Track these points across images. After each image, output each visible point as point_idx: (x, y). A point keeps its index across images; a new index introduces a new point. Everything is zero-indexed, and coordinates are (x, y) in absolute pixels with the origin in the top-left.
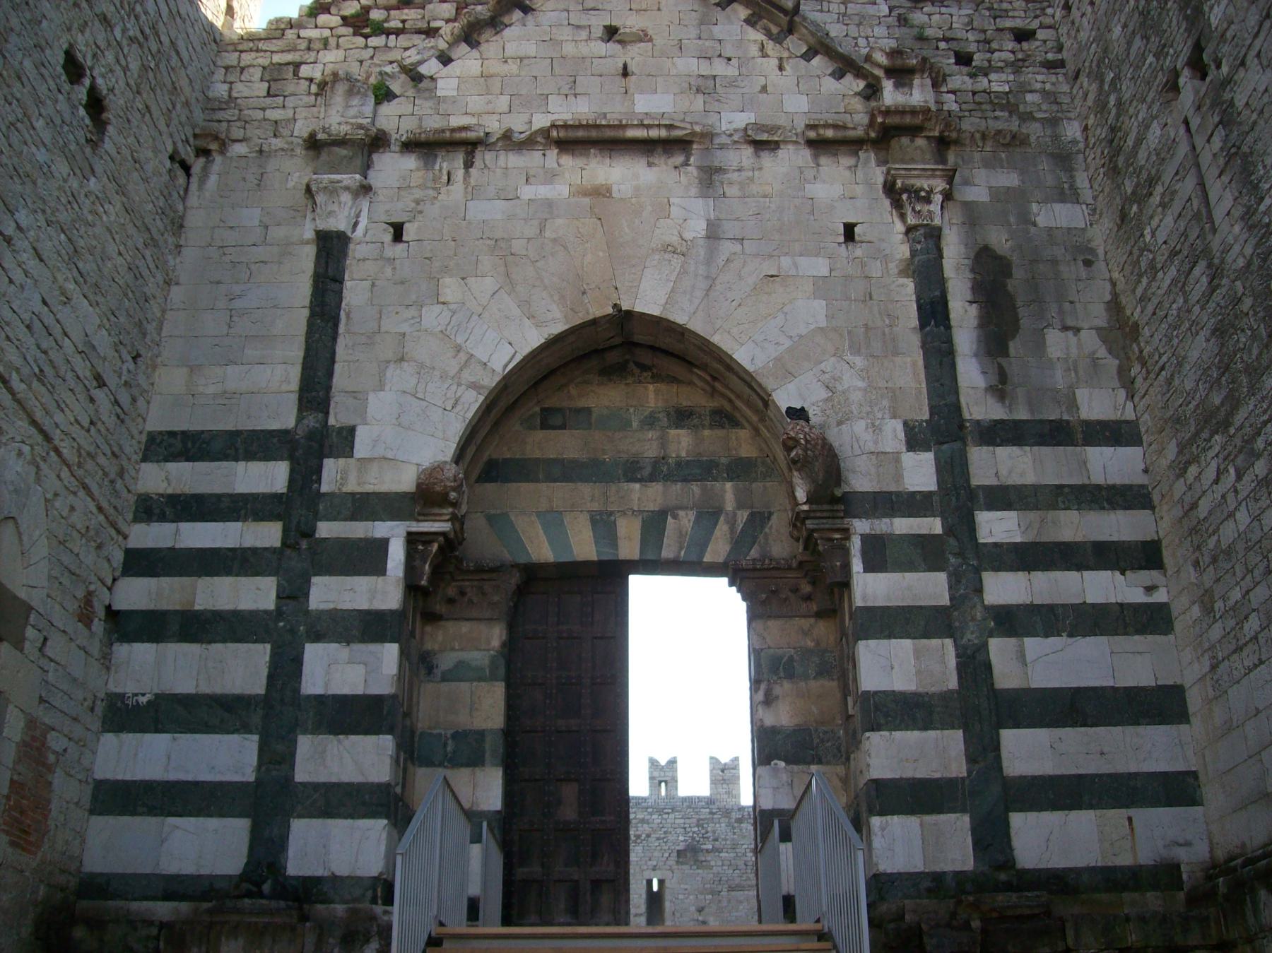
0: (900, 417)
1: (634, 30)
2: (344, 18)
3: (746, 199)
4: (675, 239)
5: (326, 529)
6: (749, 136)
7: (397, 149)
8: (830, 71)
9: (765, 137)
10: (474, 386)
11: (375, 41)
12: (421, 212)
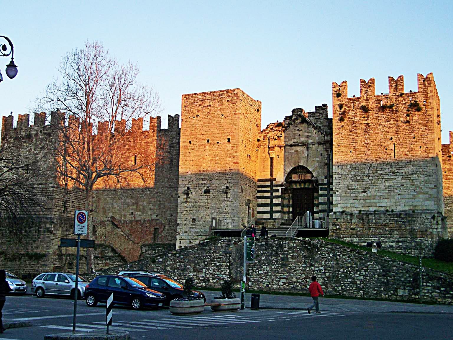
5: (274, 188)
11: (274, 132)
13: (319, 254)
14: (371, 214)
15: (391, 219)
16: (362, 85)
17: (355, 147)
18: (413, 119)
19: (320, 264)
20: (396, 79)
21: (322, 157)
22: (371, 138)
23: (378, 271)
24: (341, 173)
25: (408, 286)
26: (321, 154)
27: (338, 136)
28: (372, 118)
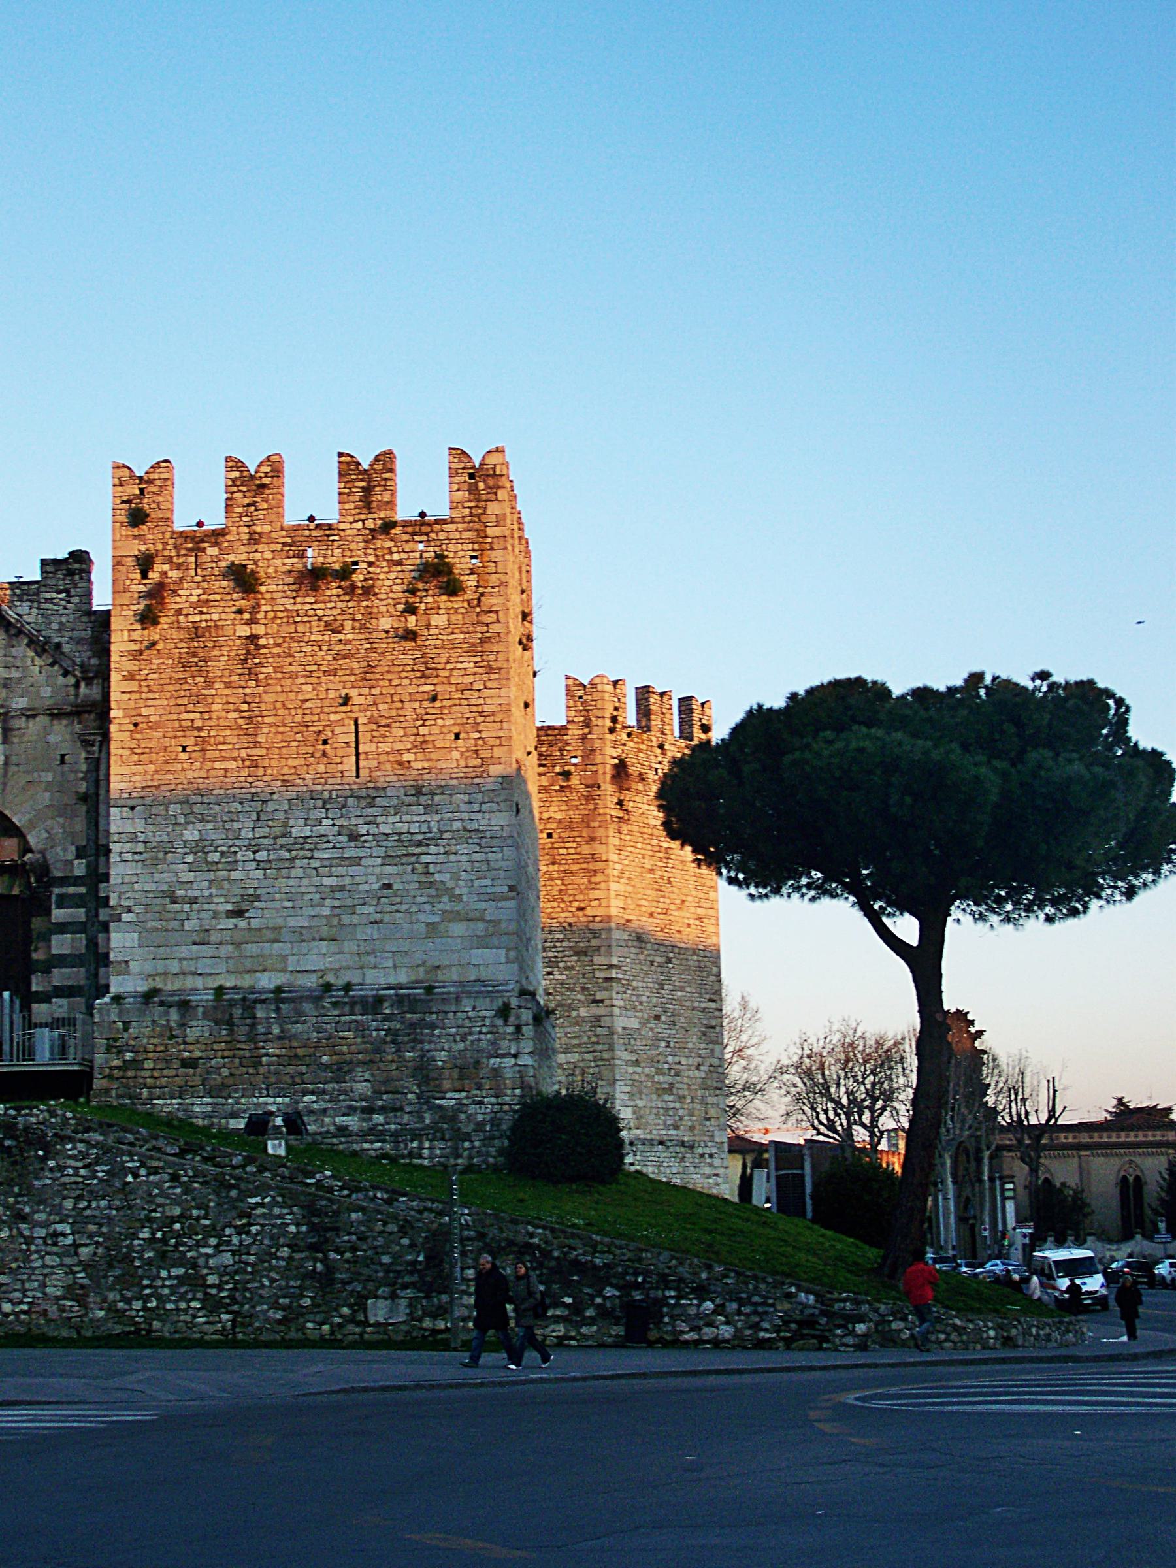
13: (51, 1170)
14: (263, 1001)
15: (343, 1018)
16: (234, 480)
17: (200, 729)
18: (428, 626)
19: (57, 1210)
20: (365, 466)
21: (66, 768)
22: (265, 697)
23: (292, 1229)
24: (141, 837)
25: (405, 1287)
26: (63, 756)
27: (133, 686)
28: (271, 615)
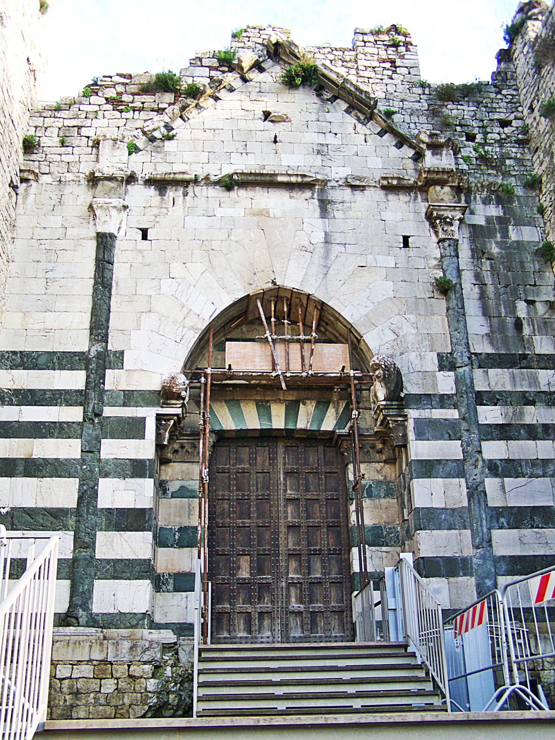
0: (435, 351)
1: (280, 114)
2: (107, 99)
3: (347, 220)
4: (306, 243)
5: (108, 411)
6: (348, 182)
7: (142, 183)
8: (394, 143)
9: (358, 183)
10: (192, 328)
12: (158, 222)
21: (411, 252)
